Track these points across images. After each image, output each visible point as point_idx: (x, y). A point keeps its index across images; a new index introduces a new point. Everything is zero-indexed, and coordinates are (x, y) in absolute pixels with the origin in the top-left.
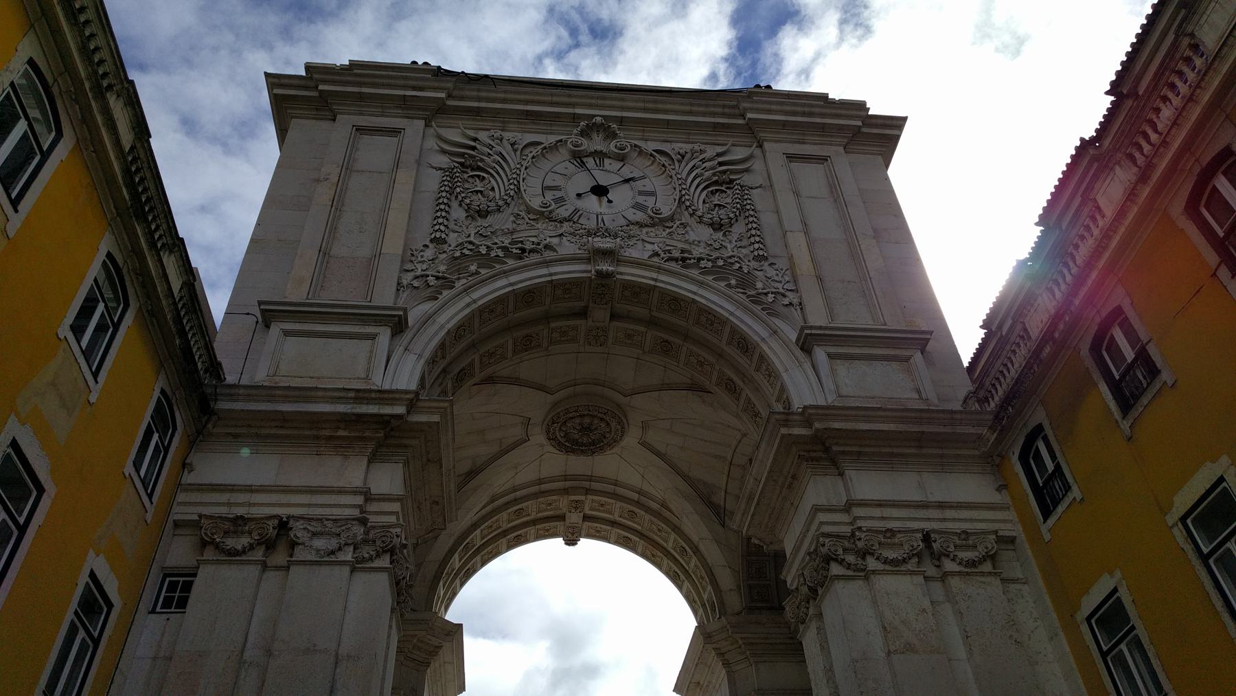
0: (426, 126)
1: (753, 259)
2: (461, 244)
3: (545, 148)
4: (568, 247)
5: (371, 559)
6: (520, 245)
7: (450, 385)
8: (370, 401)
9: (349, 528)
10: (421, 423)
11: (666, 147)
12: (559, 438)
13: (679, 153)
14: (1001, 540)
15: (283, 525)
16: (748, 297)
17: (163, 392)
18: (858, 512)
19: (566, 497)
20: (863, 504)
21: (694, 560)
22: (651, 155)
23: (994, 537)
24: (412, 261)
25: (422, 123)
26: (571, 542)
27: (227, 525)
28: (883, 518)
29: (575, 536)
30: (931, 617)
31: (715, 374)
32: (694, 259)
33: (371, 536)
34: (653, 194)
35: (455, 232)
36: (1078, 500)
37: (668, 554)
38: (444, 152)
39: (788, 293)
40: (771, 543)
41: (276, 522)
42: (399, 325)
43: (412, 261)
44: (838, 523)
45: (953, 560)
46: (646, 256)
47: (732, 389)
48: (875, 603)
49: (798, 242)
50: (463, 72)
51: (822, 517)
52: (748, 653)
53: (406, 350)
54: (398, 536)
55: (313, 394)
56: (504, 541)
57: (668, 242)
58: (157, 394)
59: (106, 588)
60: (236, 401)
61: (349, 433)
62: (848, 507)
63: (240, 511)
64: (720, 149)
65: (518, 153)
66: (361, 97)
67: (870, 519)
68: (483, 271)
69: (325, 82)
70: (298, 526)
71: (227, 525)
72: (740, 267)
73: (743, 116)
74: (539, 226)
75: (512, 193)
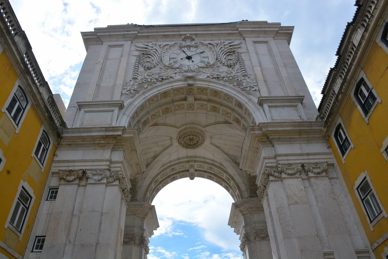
0: (132, 43)
1: (242, 76)
2: (142, 79)
3: (170, 46)
4: (178, 77)
5: (112, 182)
6: (162, 77)
7: (141, 126)
8: (110, 131)
9: (105, 172)
10: (127, 137)
11: (212, 42)
12: (183, 143)
14: (329, 165)
15: (84, 172)
16: (241, 88)
17: (44, 131)
18: (279, 158)
19: (188, 163)
20: (281, 155)
21: (232, 182)
22: (207, 45)
23: (326, 164)
24: (126, 86)
25: (130, 42)
26: (192, 178)
27: (67, 173)
28: (288, 160)
29: (193, 176)
31: (232, 117)
32: (222, 77)
33: (112, 174)
34: (208, 57)
35: (140, 75)
36: (353, 148)
37: (224, 180)
38: (137, 50)
39: (255, 87)
40: (253, 173)
41: (82, 171)
42: (121, 106)
43: (126, 86)
44: (272, 162)
45: (312, 172)
46: (205, 77)
47: (238, 121)
48: (284, 189)
49: (258, 70)
50: (144, 25)
51: (266, 161)
52: (250, 210)
53: (123, 114)
54: (121, 174)
55: (92, 130)
56: (169, 179)
57: (212, 72)
58: (41, 131)
59: (29, 192)
60: (69, 133)
61: (104, 141)
62: (275, 157)
63: (71, 168)
64: (230, 41)
65: (162, 48)
66: (110, 36)
67: (283, 161)
68: (149, 87)
69: (98, 32)
71: (67, 173)
72: (238, 79)
73: (237, 30)
74: (168, 71)
75: (159, 61)
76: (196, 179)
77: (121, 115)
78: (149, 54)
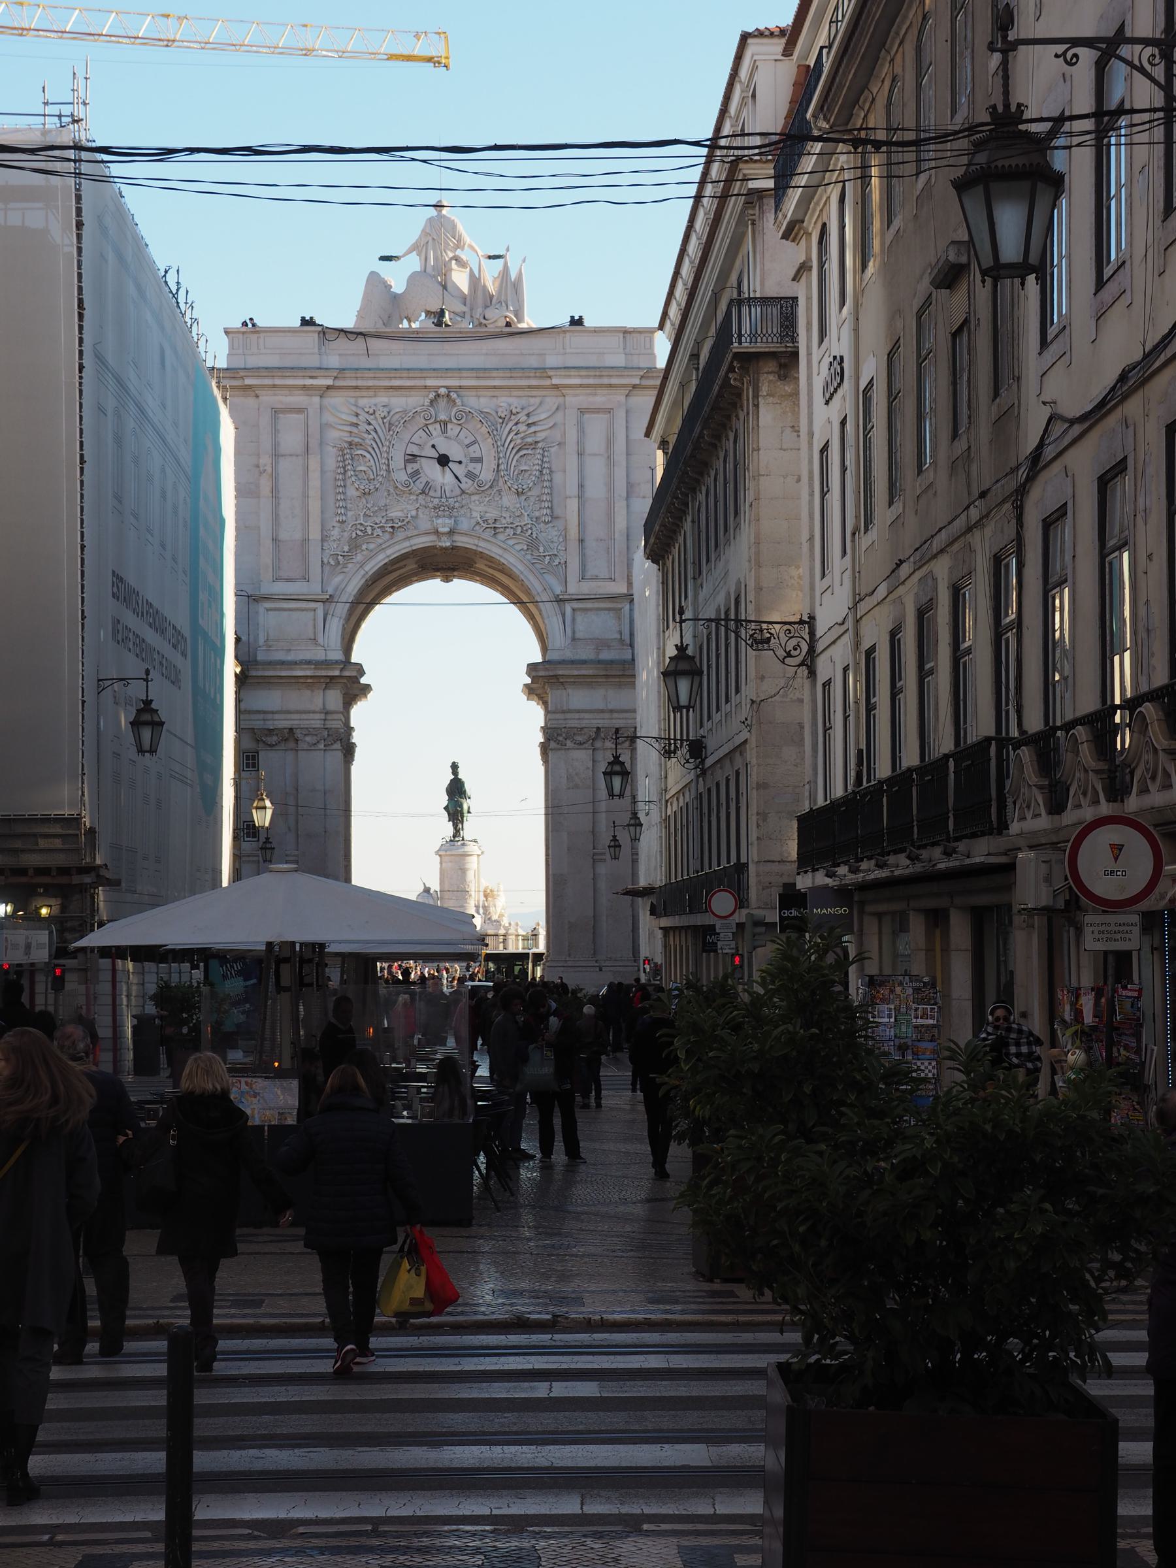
4: (424, 524)
13: (500, 417)
15: (291, 729)
18: (568, 716)
20: (569, 711)
25: (316, 399)
27: (266, 732)
30: (591, 772)
34: (479, 460)
46: (473, 522)
62: (563, 712)
66: (274, 386)
70: (298, 731)
71: (266, 732)
76: (457, 582)
77: (329, 617)
78: (359, 445)
